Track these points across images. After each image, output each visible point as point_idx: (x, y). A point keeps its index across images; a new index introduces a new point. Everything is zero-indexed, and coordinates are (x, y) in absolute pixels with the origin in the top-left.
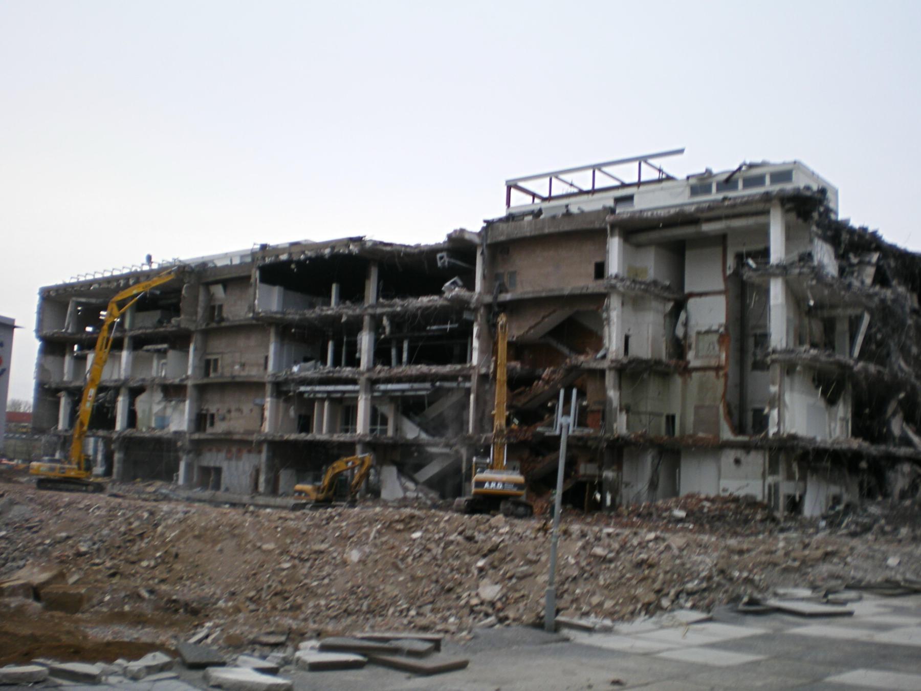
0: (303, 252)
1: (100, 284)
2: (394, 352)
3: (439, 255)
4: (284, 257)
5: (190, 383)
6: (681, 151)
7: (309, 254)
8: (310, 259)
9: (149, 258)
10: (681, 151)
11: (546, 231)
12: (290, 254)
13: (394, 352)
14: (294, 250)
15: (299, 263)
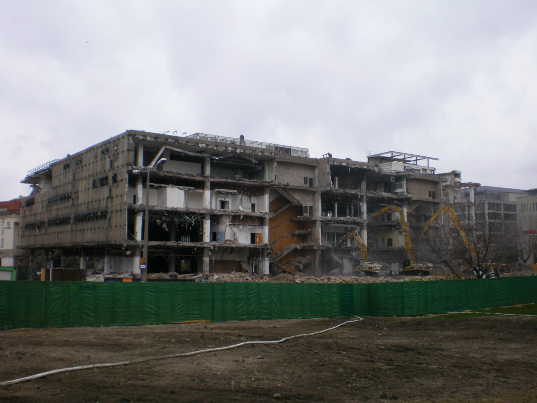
0: (354, 165)
1: (207, 145)
2: (348, 210)
3: (392, 177)
4: (344, 164)
5: (267, 217)
6: (437, 159)
7: (357, 166)
8: (357, 168)
9: (242, 137)
10: (437, 159)
11: (424, 178)
12: (348, 164)
13: (348, 210)
14: (349, 162)
15: (351, 168)
